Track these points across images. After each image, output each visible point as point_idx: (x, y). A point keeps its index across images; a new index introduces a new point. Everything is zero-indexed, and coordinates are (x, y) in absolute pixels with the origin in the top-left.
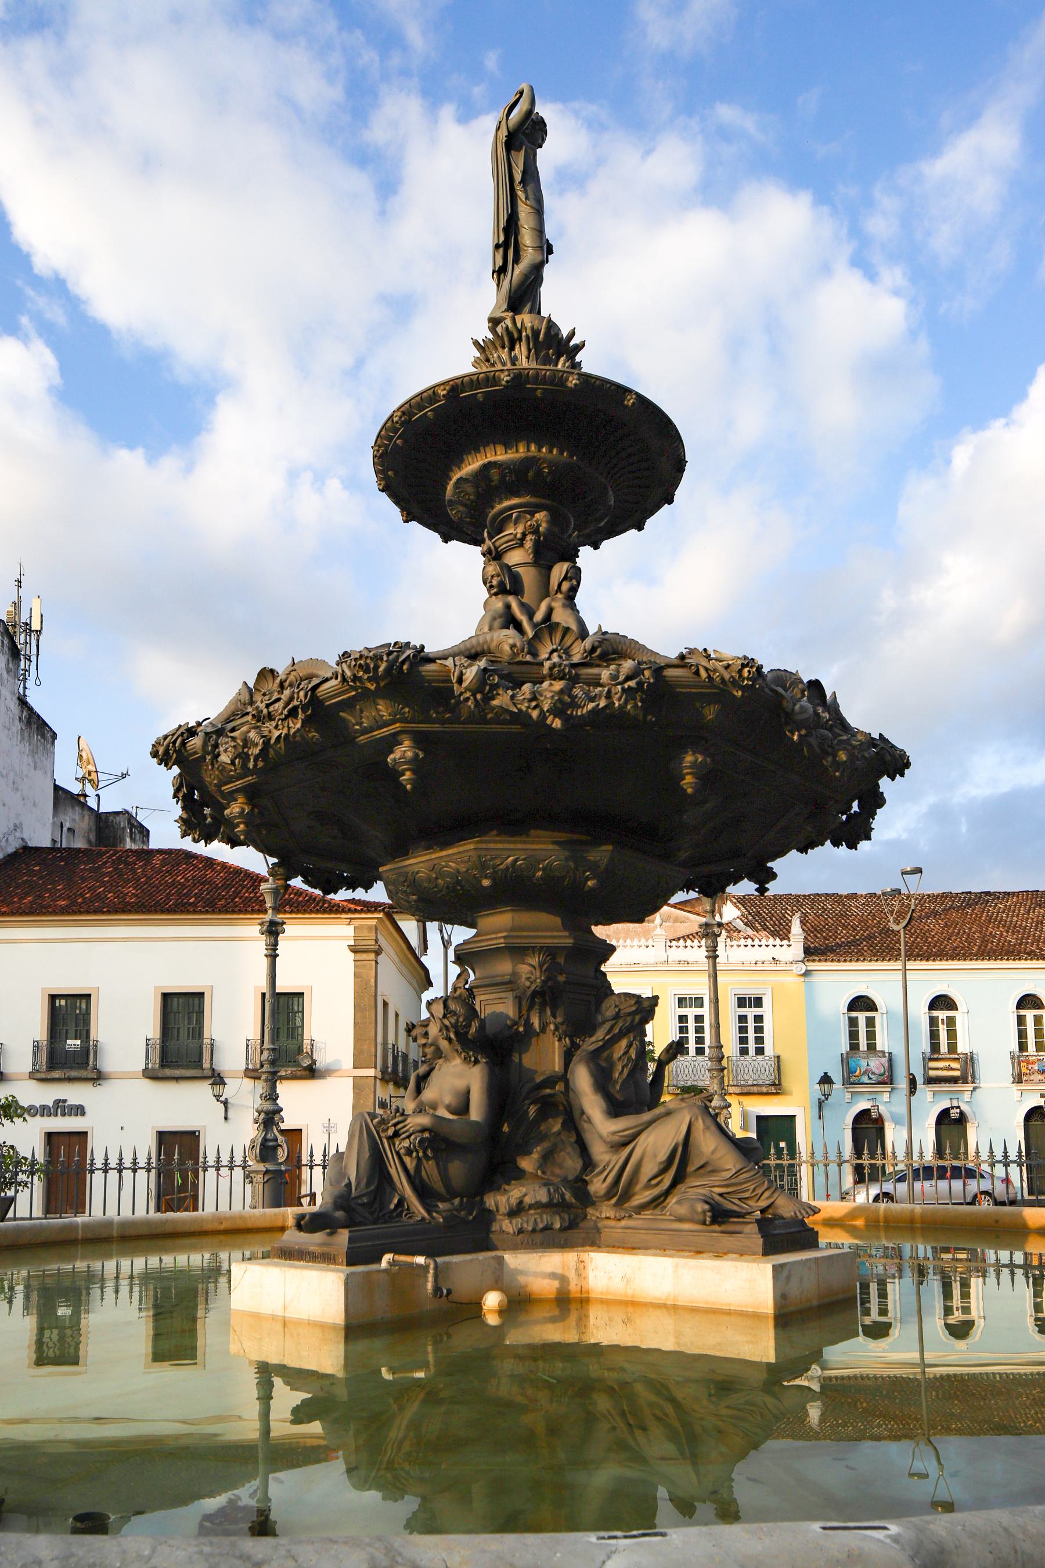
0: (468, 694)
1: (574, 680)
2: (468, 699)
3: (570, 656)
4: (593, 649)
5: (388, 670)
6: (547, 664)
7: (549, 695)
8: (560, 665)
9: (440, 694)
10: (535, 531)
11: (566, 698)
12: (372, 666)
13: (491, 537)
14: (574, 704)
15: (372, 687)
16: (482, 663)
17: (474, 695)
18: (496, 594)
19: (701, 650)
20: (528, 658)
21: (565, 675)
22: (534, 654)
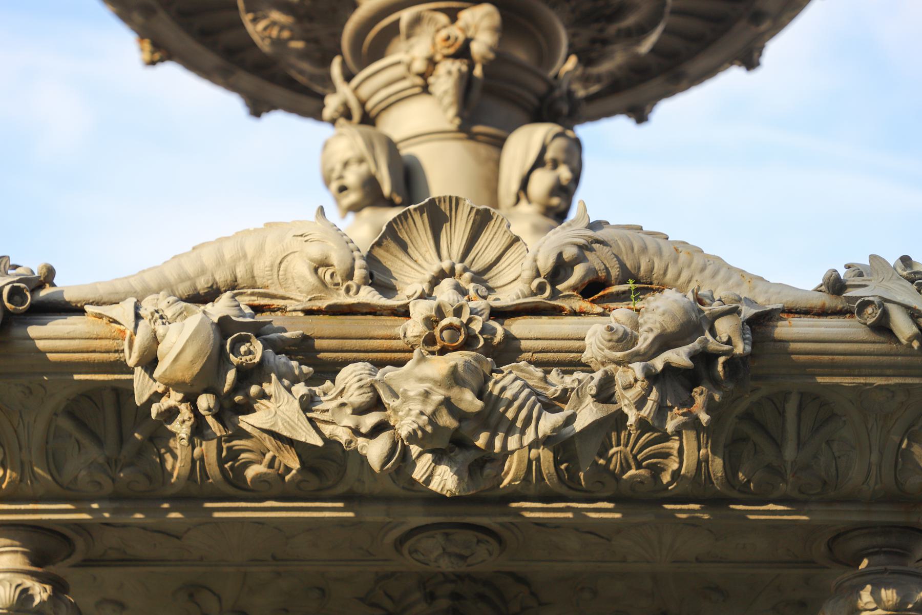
0: (174, 399)
1: (506, 352)
2: (171, 414)
4: (560, 270)
6: (420, 310)
7: (414, 389)
8: (458, 312)
9: (101, 413)
10: (463, 52)
11: (469, 401)
13: (348, 77)
14: (492, 417)
16: (220, 308)
17: (191, 399)
18: (355, 208)
19: (892, 259)
20: (368, 296)
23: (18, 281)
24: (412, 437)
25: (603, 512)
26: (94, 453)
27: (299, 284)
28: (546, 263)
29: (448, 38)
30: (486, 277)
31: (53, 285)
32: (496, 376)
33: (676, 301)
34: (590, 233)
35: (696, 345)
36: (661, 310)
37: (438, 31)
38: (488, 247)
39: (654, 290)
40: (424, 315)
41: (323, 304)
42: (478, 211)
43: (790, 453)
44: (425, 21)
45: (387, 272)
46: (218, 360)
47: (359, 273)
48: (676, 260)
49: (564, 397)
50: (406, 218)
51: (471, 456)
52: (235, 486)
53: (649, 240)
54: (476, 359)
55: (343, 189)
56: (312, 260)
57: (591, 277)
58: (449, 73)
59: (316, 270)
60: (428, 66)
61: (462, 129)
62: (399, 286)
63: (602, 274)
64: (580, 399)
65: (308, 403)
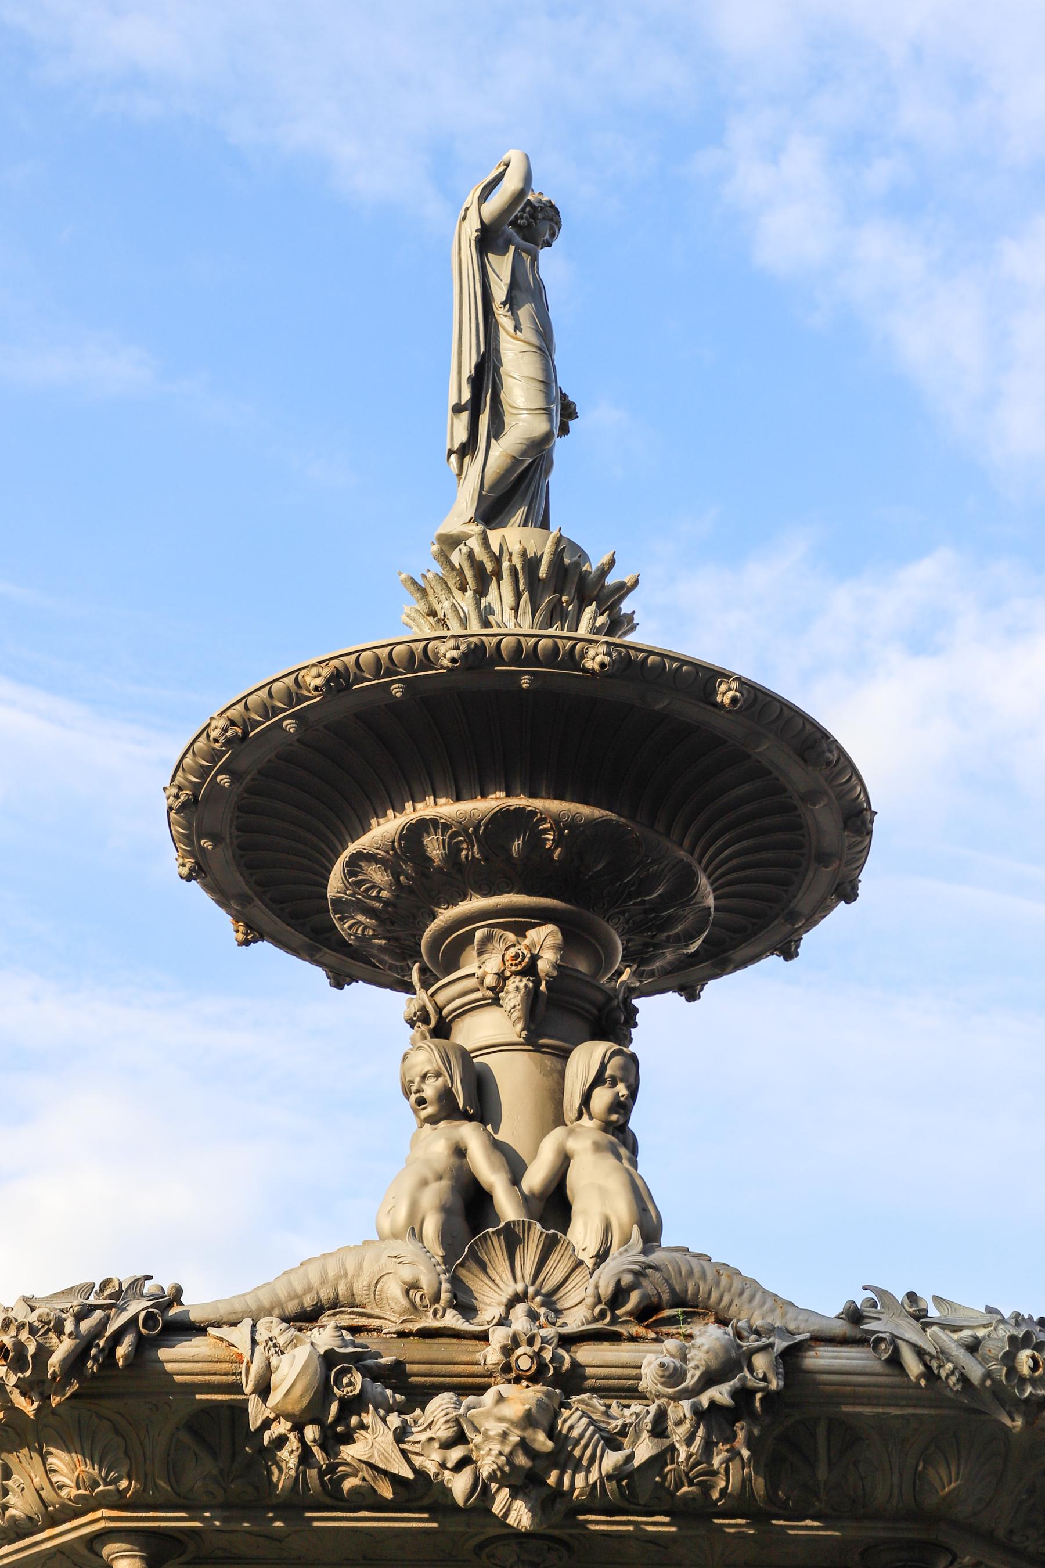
0: (282, 1427)
1: (571, 1381)
2: (281, 1441)
3: (558, 1312)
4: (619, 1295)
5: (75, 1362)
6: (499, 1337)
7: (495, 1428)
8: (531, 1342)
9: (220, 1425)
10: (530, 970)
11: (542, 1441)
12: (32, 1349)
14: (562, 1457)
15: (28, 1407)
16: (324, 1337)
17: (298, 1428)
18: (433, 1120)
20: (452, 1320)
21: (542, 1367)
22: (467, 1308)
23: (151, 1307)
24: (492, 1477)
25: (659, 1525)
26: (209, 1466)
27: (393, 1305)
28: (606, 1289)
29: (517, 956)
30: (554, 1298)
31: (181, 1304)
32: (566, 1413)
33: (718, 1339)
34: (643, 1259)
35: (735, 1382)
36: (705, 1348)
37: (507, 949)
38: (556, 1270)
39: (698, 1314)
40: (500, 1345)
41: (415, 1327)
42: (547, 1235)
43: (822, 1473)
44: (496, 938)
45: (469, 1292)
46: (323, 1392)
47: (445, 1296)
48: (718, 1284)
49: (623, 1432)
50: (486, 1240)
51: (544, 1492)
52: (334, 1498)
53: (694, 1262)
54: (547, 1395)
55: (421, 1101)
56: (404, 1283)
57: (645, 1303)
58: (517, 989)
59: (407, 1292)
60: (498, 982)
61: (528, 1041)
62: (479, 1306)
63: (655, 1300)
64: (637, 1435)
65: (401, 1435)
